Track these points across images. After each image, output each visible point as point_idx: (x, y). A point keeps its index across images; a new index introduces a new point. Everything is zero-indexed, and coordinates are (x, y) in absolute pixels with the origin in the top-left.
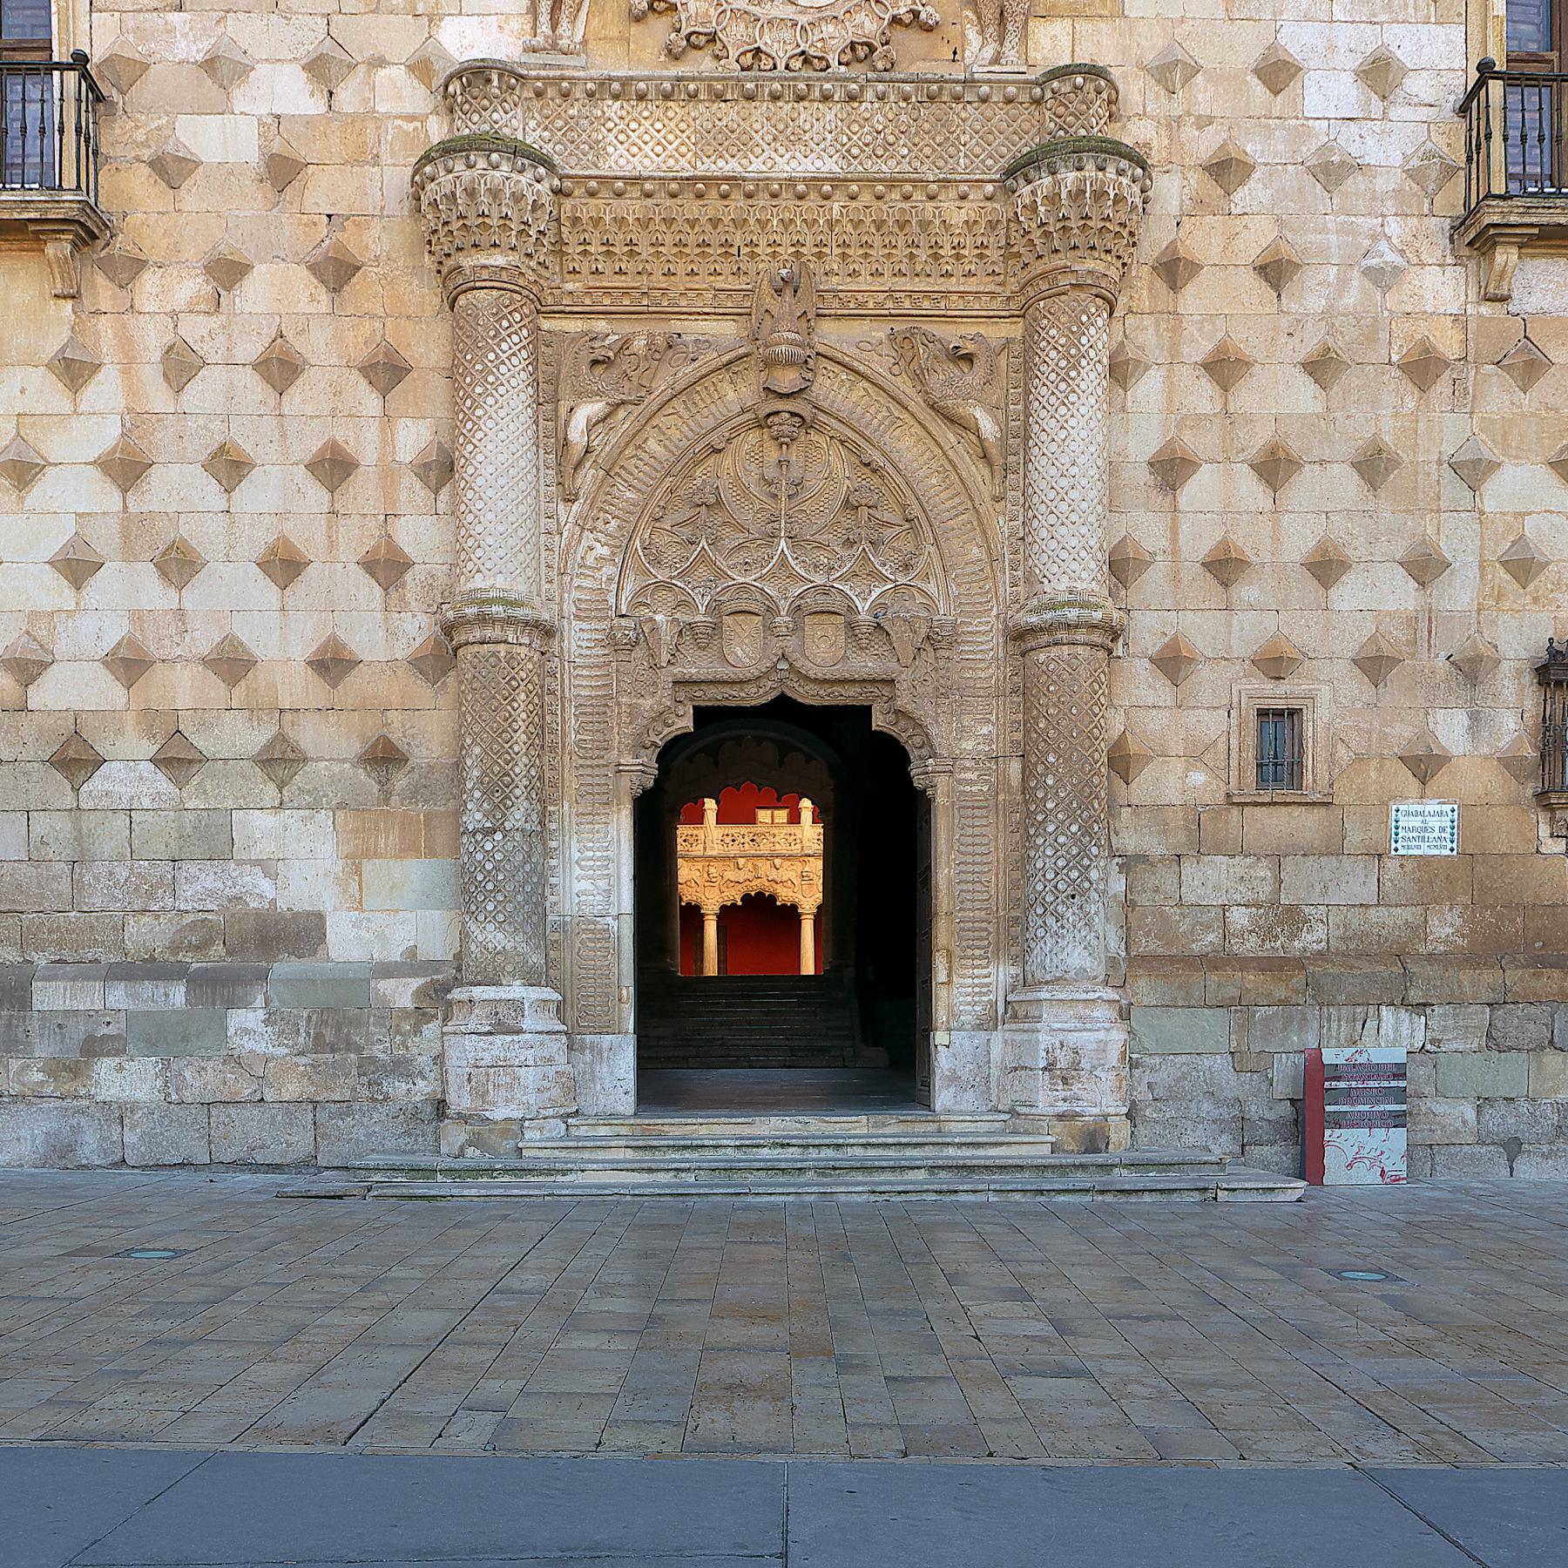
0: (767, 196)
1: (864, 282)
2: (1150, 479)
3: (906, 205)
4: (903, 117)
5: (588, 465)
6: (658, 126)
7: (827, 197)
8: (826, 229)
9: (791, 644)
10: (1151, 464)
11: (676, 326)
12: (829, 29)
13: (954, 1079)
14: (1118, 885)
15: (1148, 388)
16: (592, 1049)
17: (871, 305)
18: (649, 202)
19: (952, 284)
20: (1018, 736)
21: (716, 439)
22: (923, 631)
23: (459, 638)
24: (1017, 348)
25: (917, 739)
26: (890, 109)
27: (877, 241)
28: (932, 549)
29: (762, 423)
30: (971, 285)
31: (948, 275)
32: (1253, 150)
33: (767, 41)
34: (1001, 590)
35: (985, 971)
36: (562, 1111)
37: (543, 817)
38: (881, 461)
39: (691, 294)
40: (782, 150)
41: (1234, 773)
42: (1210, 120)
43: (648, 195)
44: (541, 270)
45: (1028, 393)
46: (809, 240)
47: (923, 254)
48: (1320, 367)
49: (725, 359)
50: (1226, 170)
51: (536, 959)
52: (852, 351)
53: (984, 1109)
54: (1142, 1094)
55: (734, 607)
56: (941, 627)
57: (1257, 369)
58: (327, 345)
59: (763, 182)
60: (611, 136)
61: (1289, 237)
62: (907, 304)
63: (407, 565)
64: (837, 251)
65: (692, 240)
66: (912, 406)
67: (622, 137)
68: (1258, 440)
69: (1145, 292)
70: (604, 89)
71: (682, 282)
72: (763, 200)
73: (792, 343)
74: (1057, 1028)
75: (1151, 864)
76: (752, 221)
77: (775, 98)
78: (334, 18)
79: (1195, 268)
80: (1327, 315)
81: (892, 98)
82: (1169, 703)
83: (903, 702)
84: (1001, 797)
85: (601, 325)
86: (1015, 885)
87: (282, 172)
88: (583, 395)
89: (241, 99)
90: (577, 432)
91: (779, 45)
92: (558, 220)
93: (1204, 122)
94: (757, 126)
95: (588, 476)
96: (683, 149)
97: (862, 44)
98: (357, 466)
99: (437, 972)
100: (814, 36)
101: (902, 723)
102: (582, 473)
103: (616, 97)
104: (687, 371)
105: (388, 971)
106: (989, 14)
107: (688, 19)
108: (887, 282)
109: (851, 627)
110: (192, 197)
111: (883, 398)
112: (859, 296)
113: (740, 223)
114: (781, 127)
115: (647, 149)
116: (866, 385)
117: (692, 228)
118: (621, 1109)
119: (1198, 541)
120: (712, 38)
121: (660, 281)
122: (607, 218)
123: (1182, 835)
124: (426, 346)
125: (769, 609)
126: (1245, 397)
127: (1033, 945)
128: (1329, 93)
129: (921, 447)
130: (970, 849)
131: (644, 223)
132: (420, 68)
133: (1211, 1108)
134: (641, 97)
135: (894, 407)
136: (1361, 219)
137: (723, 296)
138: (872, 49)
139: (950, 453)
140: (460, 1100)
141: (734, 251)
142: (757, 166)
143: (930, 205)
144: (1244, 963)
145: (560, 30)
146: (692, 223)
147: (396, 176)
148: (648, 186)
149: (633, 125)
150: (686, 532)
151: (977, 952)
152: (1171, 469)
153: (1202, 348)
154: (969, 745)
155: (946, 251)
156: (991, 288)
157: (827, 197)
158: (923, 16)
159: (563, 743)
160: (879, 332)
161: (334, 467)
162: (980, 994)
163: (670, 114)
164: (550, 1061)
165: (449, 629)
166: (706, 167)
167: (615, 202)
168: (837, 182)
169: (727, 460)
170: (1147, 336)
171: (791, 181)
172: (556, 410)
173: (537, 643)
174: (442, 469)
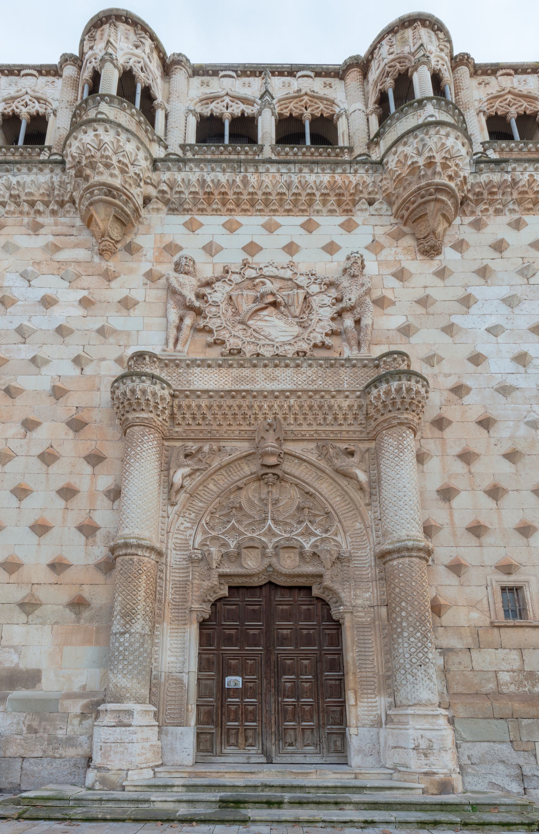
0: (262, 397)
1: (305, 427)
2: (438, 497)
3: (322, 400)
4: (320, 372)
5: (182, 492)
6: (216, 375)
7: (288, 397)
8: (287, 408)
9: (274, 560)
10: (438, 491)
11: (222, 444)
12: (287, 347)
13: (360, 751)
14: (440, 661)
15: (433, 465)
16: (172, 734)
17: (308, 435)
18: (212, 400)
19: (344, 428)
20: (385, 597)
21: (239, 484)
22: (336, 556)
23: (116, 554)
24: (373, 451)
25: (334, 600)
26: (314, 369)
27: (310, 413)
28: (338, 524)
29: (260, 478)
30: (352, 428)
31: (341, 425)
32: (469, 382)
33: (262, 351)
34: (371, 540)
35: (374, 700)
36: (152, 764)
37: (153, 629)
38: (314, 491)
39: (229, 432)
40: (268, 383)
41: (493, 613)
42: (450, 375)
43: (211, 397)
44: (164, 422)
45: (378, 465)
46: (280, 413)
47: (330, 417)
48: (512, 456)
49: (244, 454)
50: (459, 390)
51: (145, 692)
52: (299, 452)
53: (378, 766)
54: (465, 760)
55: (247, 545)
56: (344, 553)
57: (482, 457)
58: (70, 447)
59: (260, 392)
60: (196, 379)
61: (490, 412)
62: (323, 435)
63: (97, 528)
64: (292, 416)
65: (229, 413)
66: (327, 471)
67: (201, 379)
68: (487, 483)
69: (428, 431)
70: (193, 363)
71: (225, 428)
72: (260, 398)
73: (273, 447)
74: (415, 731)
75: (456, 652)
76: (256, 406)
77: (265, 366)
78: (86, 346)
79: (450, 422)
80: (511, 438)
81: (315, 366)
82: (457, 584)
83: (327, 582)
84: (377, 623)
85: (190, 444)
86: (387, 662)
87: (58, 393)
88: (180, 466)
89: (44, 370)
90: (177, 478)
91: (267, 352)
92: (172, 406)
93: (447, 376)
94: (258, 375)
95: (182, 497)
96: (226, 383)
97: (302, 352)
98: (79, 492)
99: (94, 696)
100: (281, 349)
101: (327, 593)
102: (179, 495)
103: (199, 366)
104: (227, 459)
105: (70, 696)
106: (353, 342)
107: (230, 345)
108: (315, 427)
109: (302, 555)
110: (19, 401)
111: (313, 469)
112: (303, 433)
113: (250, 407)
114: (268, 375)
115: (211, 383)
116: (306, 464)
117: (230, 408)
118: (185, 763)
119: (463, 520)
120: (239, 351)
121: (215, 427)
122: (193, 405)
123: (470, 640)
124: (112, 451)
125: (263, 547)
126: (477, 467)
127: (399, 688)
128: (500, 366)
129: (331, 487)
130: (363, 645)
131: (210, 407)
132: (119, 361)
133: (504, 768)
134: (209, 366)
135: (320, 473)
136: (521, 406)
137: (243, 432)
138: (305, 353)
139: (345, 488)
140: (97, 760)
141: (248, 416)
142: (258, 387)
143: (332, 400)
144: (511, 696)
145: (177, 348)
146: (230, 407)
147: (105, 395)
148: (211, 393)
149: (206, 375)
150: (225, 519)
151: (369, 691)
152: (447, 494)
153: (458, 450)
154: (359, 602)
155: (340, 416)
156: (361, 429)
157: (288, 397)
158: (327, 343)
159: (165, 599)
160: (312, 445)
161: (68, 493)
162: (372, 711)
163: (221, 371)
164: (147, 740)
165: (113, 550)
166: (237, 388)
167: (197, 400)
168: (292, 392)
169: (243, 493)
170: (431, 446)
171: (273, 392)
172: (169, 473)
173: (153, 556)
174: (115, 494)
